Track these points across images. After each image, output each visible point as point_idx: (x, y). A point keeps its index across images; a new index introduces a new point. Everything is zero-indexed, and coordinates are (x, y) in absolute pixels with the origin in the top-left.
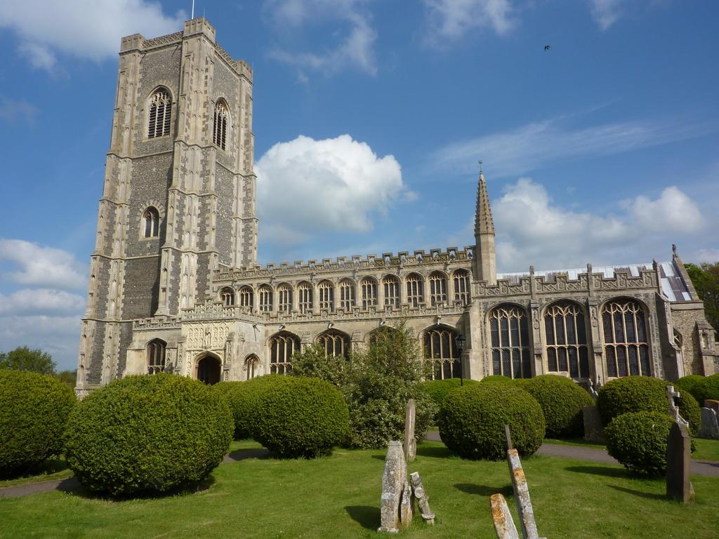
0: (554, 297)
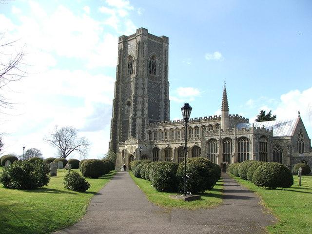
0: (225, 137)
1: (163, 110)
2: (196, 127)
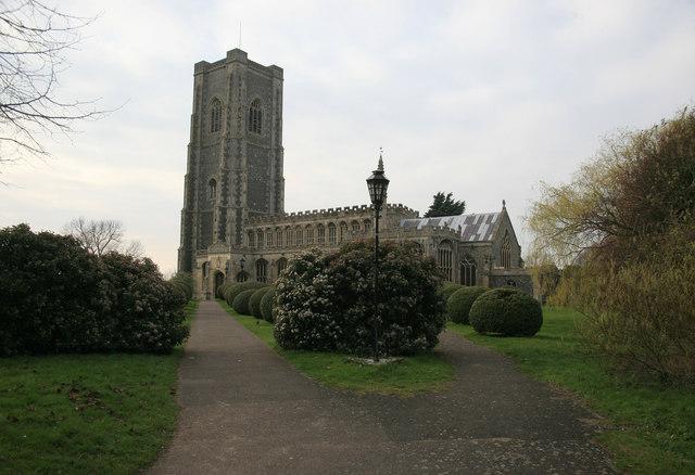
1: (272, 195)
2: (331, 224)
